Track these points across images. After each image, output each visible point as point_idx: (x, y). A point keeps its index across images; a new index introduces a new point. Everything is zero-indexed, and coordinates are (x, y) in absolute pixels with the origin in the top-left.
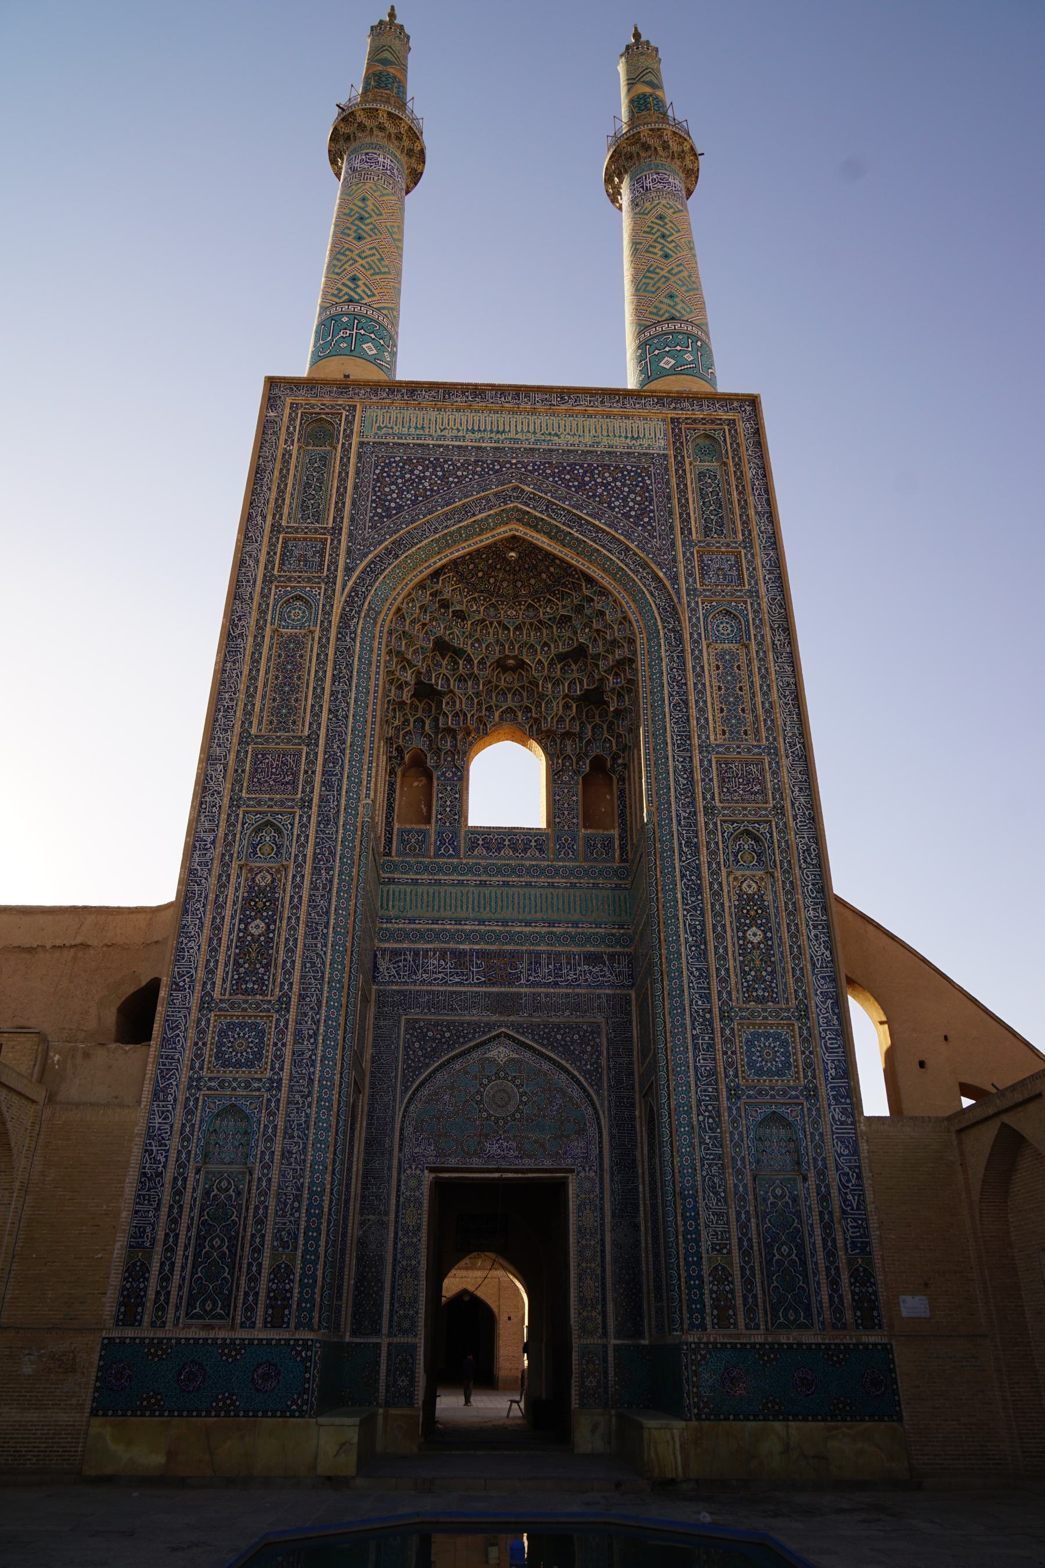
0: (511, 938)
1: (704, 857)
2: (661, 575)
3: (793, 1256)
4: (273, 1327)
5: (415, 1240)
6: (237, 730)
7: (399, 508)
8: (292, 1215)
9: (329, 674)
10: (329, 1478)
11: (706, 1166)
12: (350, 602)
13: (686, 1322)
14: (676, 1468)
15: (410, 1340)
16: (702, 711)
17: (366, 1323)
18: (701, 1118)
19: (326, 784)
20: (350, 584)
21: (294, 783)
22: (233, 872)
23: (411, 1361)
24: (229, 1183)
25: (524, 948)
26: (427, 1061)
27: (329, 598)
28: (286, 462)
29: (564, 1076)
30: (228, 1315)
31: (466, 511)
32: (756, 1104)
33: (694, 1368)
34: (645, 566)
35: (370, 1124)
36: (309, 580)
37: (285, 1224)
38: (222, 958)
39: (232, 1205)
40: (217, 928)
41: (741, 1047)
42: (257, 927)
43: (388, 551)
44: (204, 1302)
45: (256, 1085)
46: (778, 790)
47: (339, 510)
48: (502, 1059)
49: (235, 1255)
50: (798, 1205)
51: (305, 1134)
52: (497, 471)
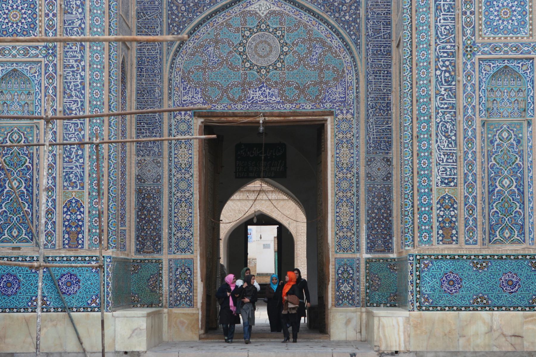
3: (513, 188)
5: (187, 176)
8: (77, 161)
10: (126, 353)
11: (440, 114)
13: (417, 239)
14: (399, 344)
15: (188, 255)
17: (149, 243)
18: (438, 73)
23: (189, 273)
24: (20, 136)
26: (190, 15)
29: (323, 27)
30: (32, 240)
32: (490, 60)
33: (418, 273)
35: (140, 76)
37: (71, 168)
39: (25, 154)
41: (480, 8)
44: (11, 230)
45: (34, 52)
48: (263, 12)
49: (32, 194)
50: (522, 145)
51: (82, 94)
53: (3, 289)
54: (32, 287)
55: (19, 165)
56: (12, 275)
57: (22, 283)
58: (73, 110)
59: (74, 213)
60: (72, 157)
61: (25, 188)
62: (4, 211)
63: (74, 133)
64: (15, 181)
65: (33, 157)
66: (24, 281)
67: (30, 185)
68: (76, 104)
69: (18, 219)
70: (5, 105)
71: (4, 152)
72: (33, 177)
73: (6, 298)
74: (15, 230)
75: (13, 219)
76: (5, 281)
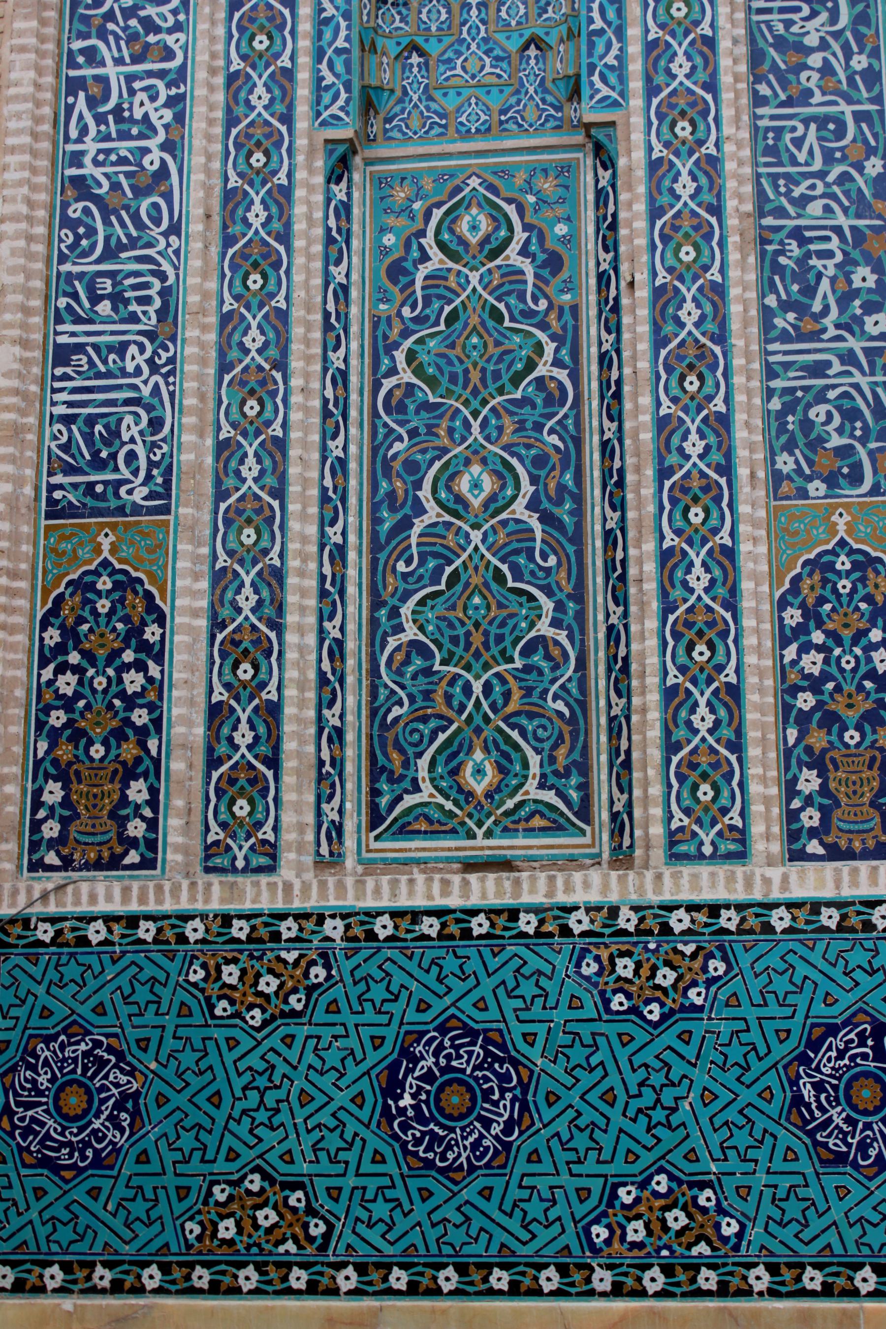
4: (834, 853)
24: (499, 218)
30: (584, 812)
37: (818, 369)
39: (529, 314)
44: (453, 756)
49: (578, 538)
53: (418, 1129)
54: (615, 1114)
55: (497, 375)
56: (473, 1034)
57: (546, 1084)
58: (810, 51)
59: (847, 635)
60: (817, 307)
61: (533, 505)
62: (414, 644)
63: (821, 175)
64: (476, 469)
65: (576, 329)
66: (557, 1070)
67: (562, 488)
68: (824, 16)
69: (498, 689)
70: (415, 59)
71: (406, 312)
72: (578, 442)
73: (441, 1193)
74: (478, 755)
75: (467, 689)
76: (428, 1077)
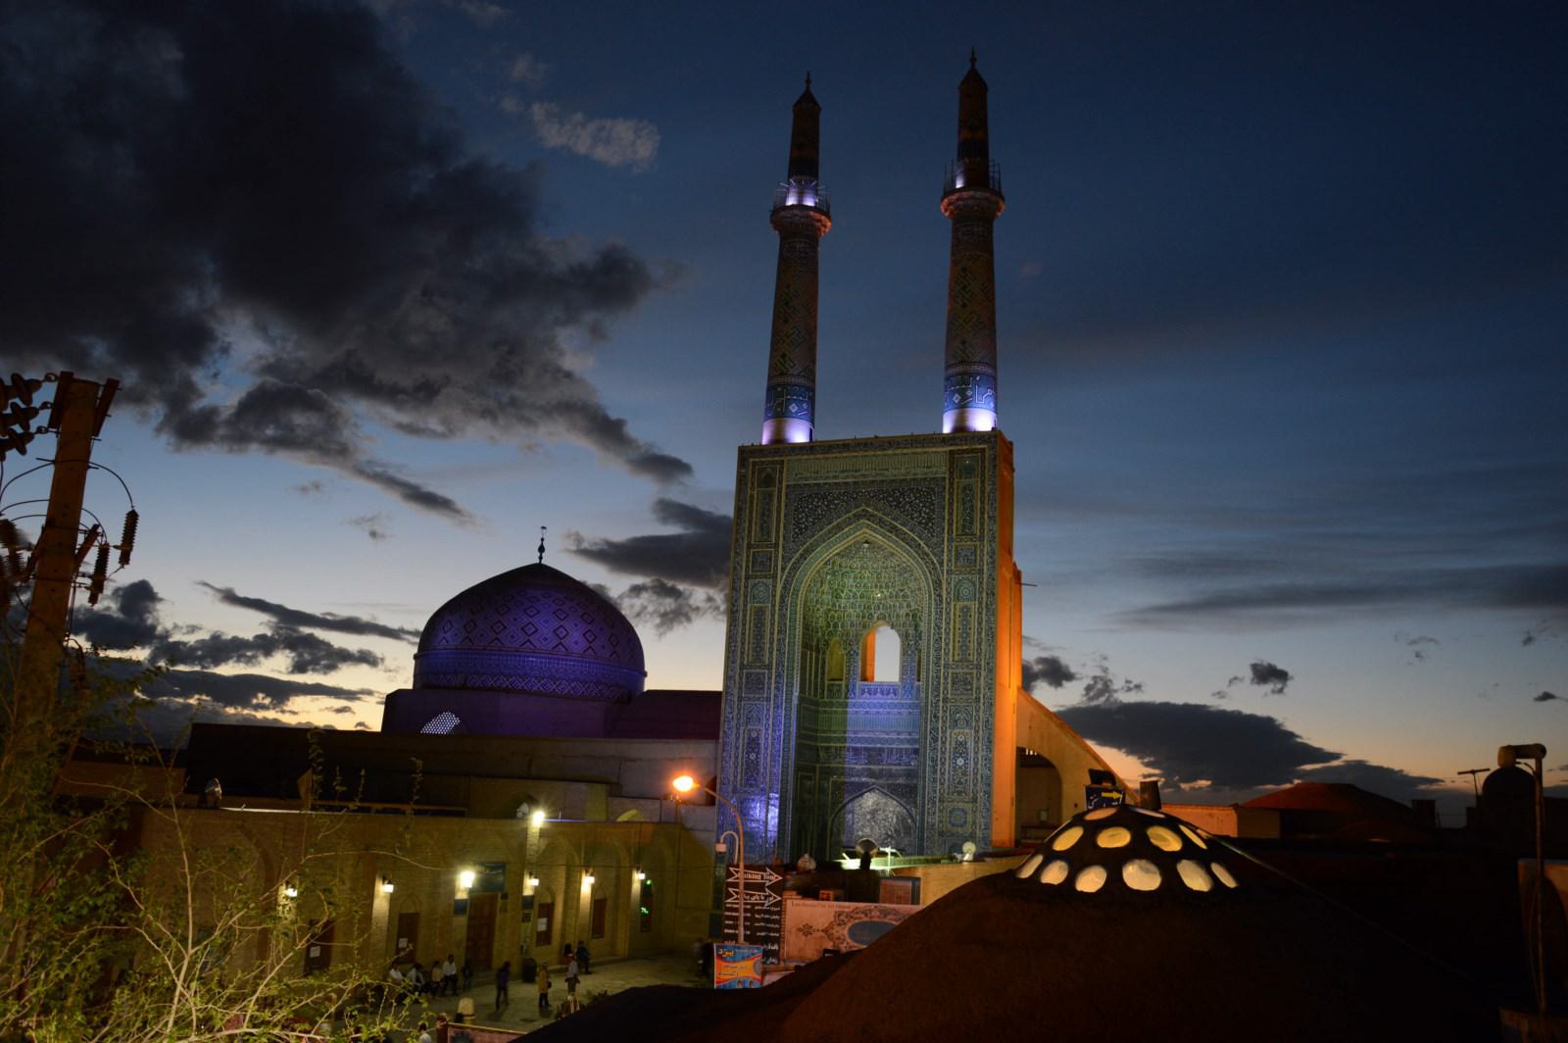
0: (880, 740)
1: (940, 725)
2: (935, 561)
6: (738, 662)
7: (806, 528)
9: (776, 631)
12: (784, 588)
16: (947, 644)
19: (777, 688)
20: (784, 577)
21: (763, 688)
22: (741, 731)
25: (885, 746)
27: (775, 586)
28: (752, 503)
31: (839, 528)
34: (928, 555)
36: (765, 577)
38: (739, 770)
40: (737, 758)
42: (753, 756)
43: (801, 555)
46: (978, 688)
47: (778, 532)
52: (854, 499)
